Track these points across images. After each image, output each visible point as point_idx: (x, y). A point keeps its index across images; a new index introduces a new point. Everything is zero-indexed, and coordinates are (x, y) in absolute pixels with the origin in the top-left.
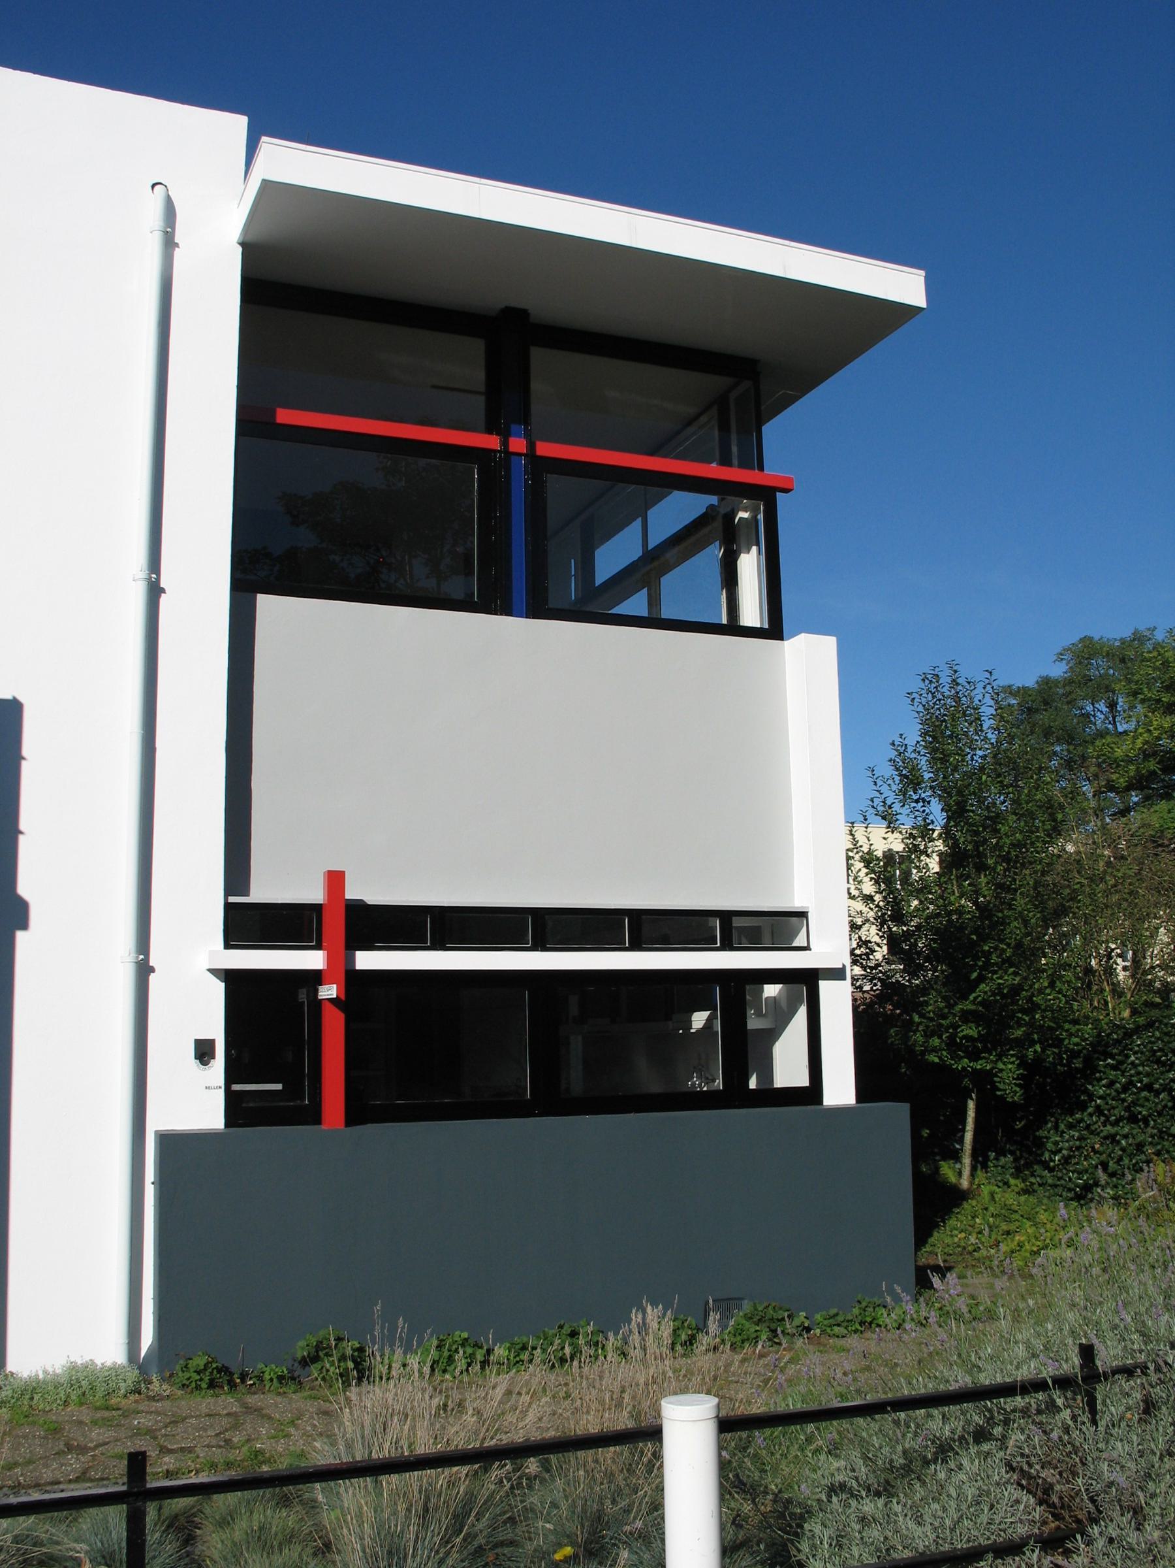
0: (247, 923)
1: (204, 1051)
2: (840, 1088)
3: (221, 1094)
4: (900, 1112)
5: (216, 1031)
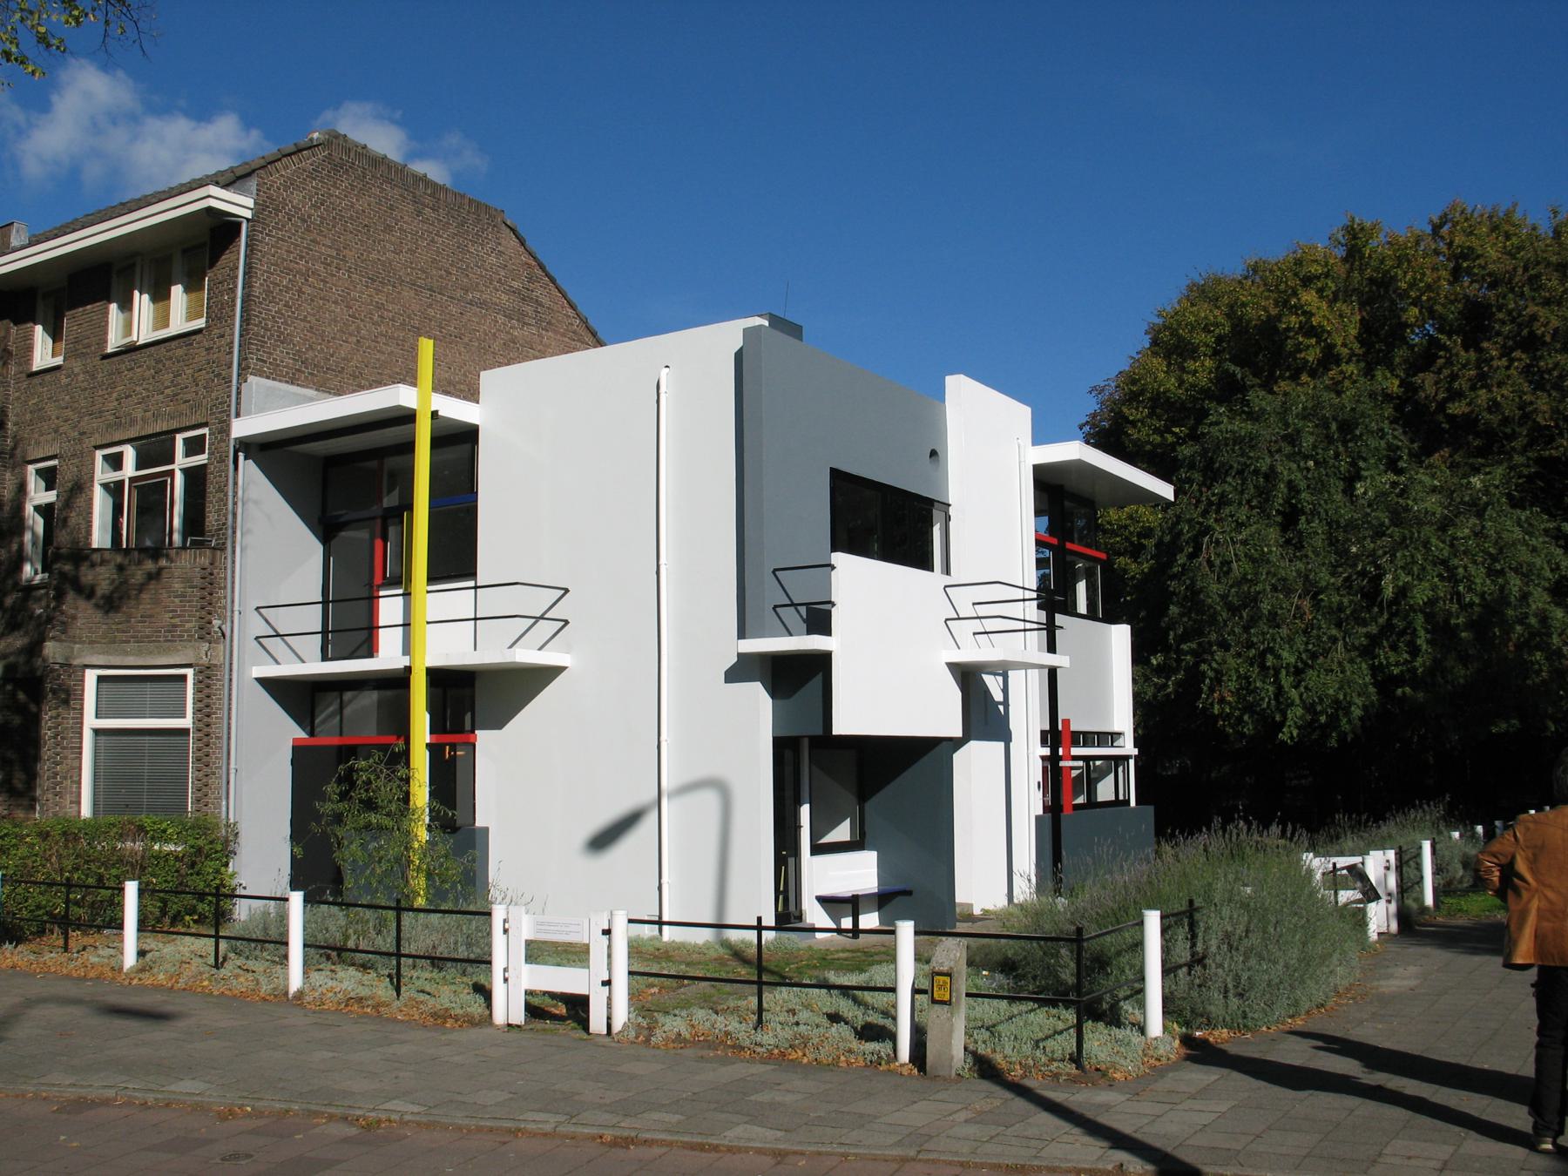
4: (1150, 809)
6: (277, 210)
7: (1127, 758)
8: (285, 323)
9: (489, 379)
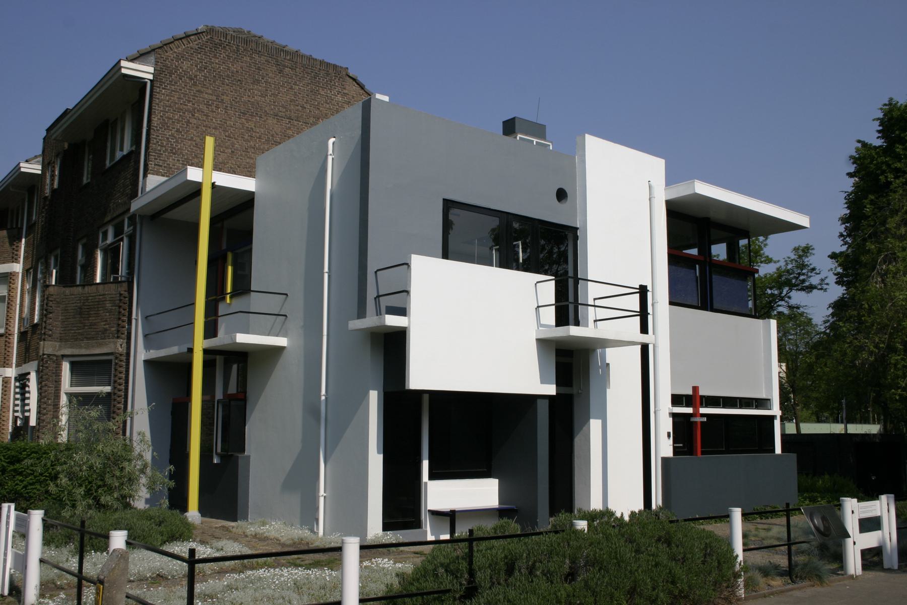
0: (677, 400)
1: (669, 434)
2: (778, 450)
3: (671, 448)
4: (793, 456)
6: (171, 74)
7: (772, 418)
8: (177, 142)
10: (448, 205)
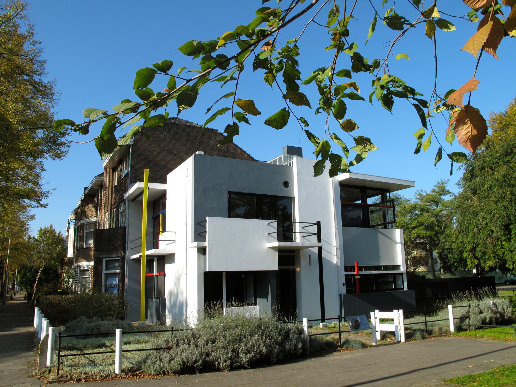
0: (347, 269)
1: (343, 284)
5: (345, 282)
7: (402, 274)
9: (170, 177)
10: (230, 193)
